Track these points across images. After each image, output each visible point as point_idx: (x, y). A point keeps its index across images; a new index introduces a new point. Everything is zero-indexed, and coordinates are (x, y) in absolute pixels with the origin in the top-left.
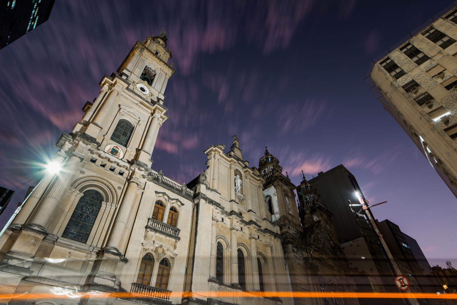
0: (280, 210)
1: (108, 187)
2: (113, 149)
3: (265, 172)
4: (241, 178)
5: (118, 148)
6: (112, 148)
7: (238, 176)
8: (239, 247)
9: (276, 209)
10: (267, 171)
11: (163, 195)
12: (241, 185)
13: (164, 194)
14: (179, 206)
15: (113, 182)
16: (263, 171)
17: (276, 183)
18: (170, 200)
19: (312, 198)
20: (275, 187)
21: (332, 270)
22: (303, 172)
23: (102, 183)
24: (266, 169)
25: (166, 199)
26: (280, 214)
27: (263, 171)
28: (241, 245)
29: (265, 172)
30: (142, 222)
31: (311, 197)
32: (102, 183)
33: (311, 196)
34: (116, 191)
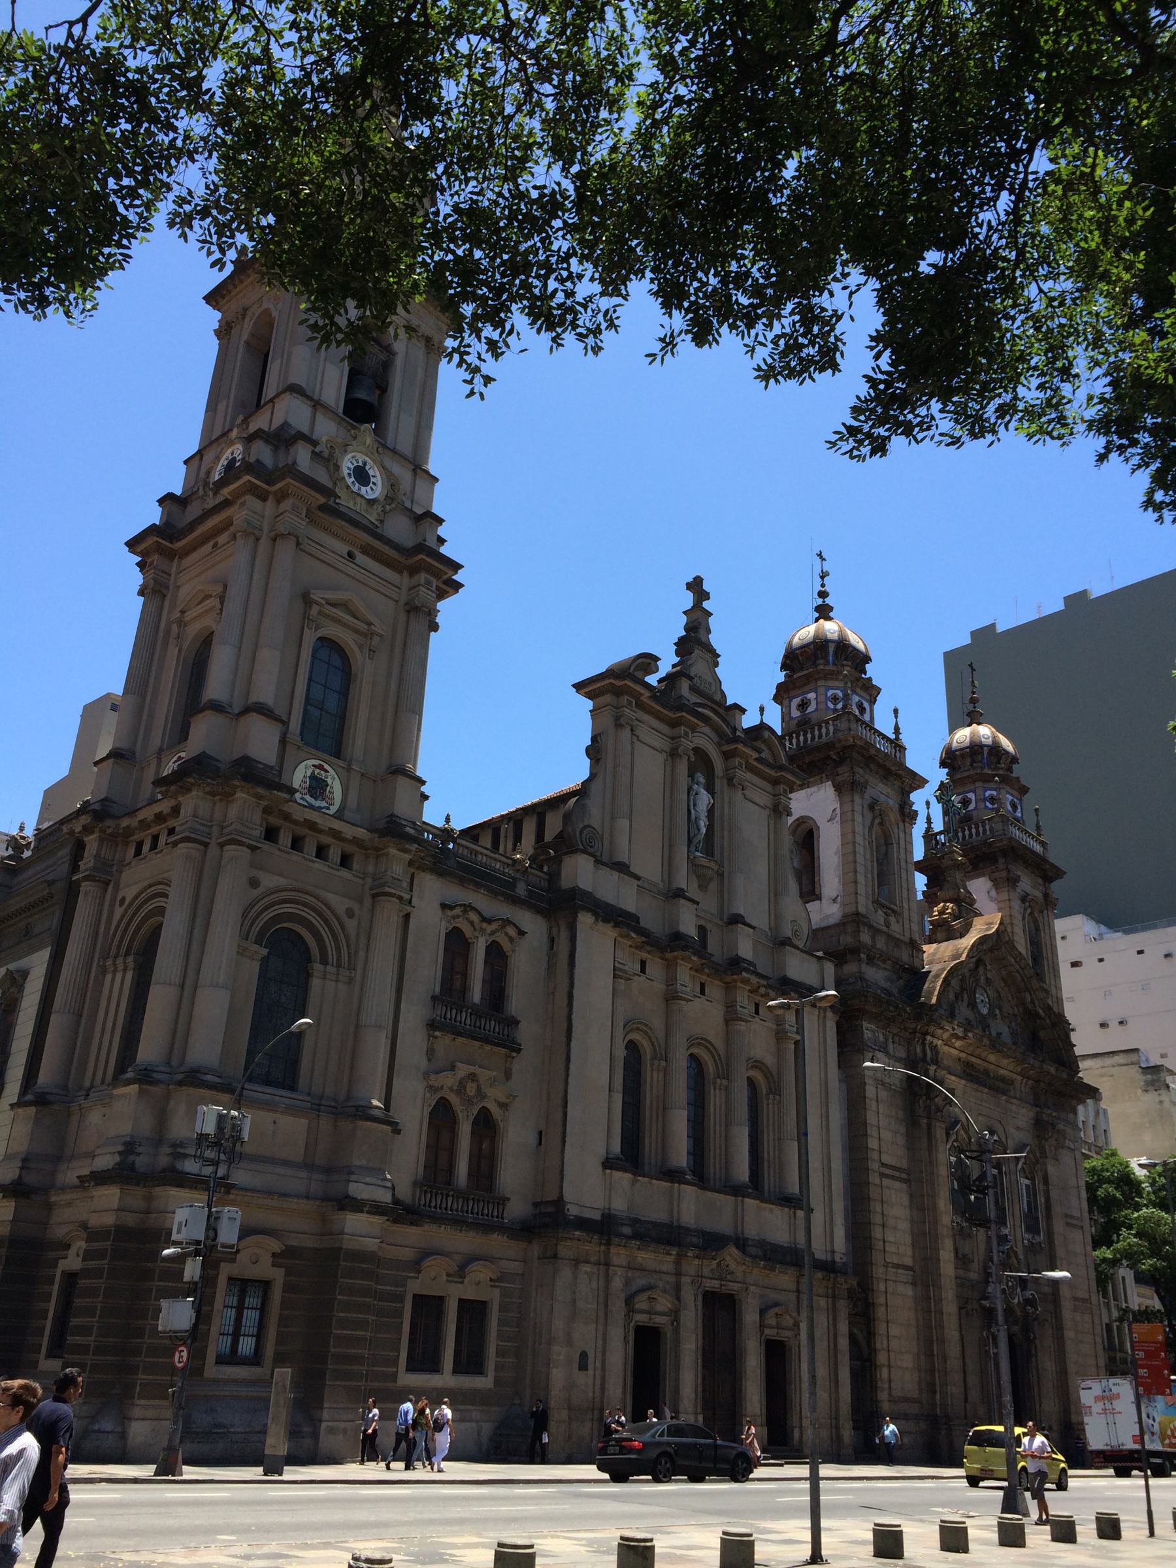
0: (844, 890)
1: (320, 914)
2: (313, 777)
3: (803, 705)
4: (710, 789)
5: (326, 771)
6: (309, 774)
7: (701, 778)
8: (691, 1051)
9: (831, 880)
11: (465, 912)
12: (711, 812)
13: (467, 908)
14: (511, 939)
15: (332, 898)
16: (796, 702)
17: (844, 773)
18: (484, 925)
19: (988, 804)
20: (838, 788)
21: (1004, 1098)
22: (973, 670)
23: (306, 905)
24: (812, 696)
25: (472, 923)
26: (843, 905)
27: (796, 702)
28: (699, 1044)
29: (803, 705)
30: (414, 1015)
31: (985, 800)
32: (306, 905)
33: (988, 794)
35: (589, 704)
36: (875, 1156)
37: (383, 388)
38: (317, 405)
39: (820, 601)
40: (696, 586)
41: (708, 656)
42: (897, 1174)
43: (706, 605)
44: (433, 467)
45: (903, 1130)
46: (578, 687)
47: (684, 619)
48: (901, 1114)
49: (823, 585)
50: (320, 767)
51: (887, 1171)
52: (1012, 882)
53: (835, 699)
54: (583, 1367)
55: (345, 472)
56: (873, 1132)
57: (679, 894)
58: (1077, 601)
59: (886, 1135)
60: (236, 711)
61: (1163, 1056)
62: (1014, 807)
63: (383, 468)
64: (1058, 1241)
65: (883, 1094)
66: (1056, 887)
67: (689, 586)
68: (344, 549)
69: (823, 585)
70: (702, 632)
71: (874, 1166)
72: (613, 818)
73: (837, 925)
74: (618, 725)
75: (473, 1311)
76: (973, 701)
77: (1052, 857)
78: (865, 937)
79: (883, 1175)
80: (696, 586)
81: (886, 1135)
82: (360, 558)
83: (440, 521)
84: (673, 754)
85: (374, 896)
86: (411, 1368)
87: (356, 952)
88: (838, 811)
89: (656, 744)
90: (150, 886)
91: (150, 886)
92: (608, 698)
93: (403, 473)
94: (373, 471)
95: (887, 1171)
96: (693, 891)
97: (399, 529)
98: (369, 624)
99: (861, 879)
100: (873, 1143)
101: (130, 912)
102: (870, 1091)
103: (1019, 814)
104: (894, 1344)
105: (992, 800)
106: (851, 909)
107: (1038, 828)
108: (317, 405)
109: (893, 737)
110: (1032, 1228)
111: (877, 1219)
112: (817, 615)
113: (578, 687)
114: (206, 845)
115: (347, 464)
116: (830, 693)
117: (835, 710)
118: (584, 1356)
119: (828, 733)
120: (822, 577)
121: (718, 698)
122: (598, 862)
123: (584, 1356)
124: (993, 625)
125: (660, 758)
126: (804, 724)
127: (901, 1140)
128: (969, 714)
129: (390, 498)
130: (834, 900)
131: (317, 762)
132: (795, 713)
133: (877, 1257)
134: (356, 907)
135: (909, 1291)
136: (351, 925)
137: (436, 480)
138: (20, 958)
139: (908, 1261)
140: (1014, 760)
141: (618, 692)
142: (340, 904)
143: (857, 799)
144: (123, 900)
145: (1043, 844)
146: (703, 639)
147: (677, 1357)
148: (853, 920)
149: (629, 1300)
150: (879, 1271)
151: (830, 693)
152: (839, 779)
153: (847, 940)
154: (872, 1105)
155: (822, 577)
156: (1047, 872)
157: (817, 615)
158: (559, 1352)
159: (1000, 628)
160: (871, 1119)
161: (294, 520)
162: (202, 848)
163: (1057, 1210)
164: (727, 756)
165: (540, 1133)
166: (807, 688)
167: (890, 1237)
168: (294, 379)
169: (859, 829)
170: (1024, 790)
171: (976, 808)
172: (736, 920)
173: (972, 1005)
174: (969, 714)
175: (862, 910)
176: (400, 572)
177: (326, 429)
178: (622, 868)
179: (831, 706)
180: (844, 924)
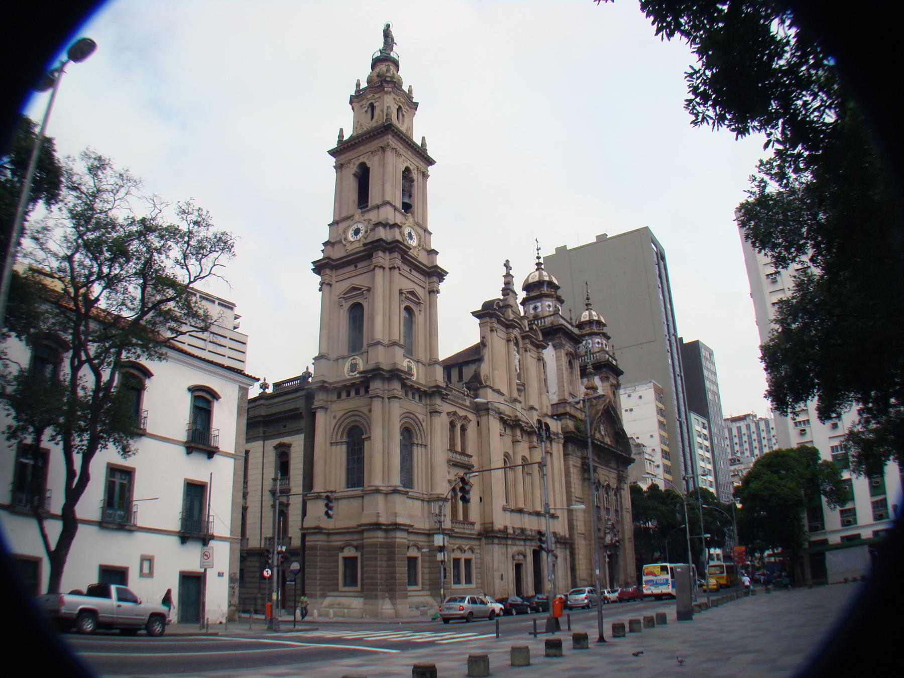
3: (535, 308)
4: (518, 352)
10: (539, 310)
12: (519, 362)
13: (455, 413)
16: (532, 306)
17: (557, 341)
24: (539, 304)
26: (559, 395)
27: (532, 306)
29: (535, 308)
33: (597, 340)
34: (422, 426)
35: (478, 321)
36: (573, 494)
37: (410, 196)
38: (395, 209)
39: (537, 261)
40: (507, 265)
41: (514, 295)
42: (579, 500)
43: (511, 272)
44: (430, 230)
45: (581, 483)
46: (474, 313)
47: (503, 279)
48: (580, 477)
49: (538, 254)
50: (409, 362)
51: (577, 499)
52: (607, 378)
53: (549, 306)
54: (502, 579)
55: (406, 235)
56: (573, 485)
57: (516, 400)
58: (602, 238)
59: (576, 486)
60: (386, 342)
61: (638, 438)
62: (606, 346)
63: (416, 232)
64: (624, 518)
65: (575, 470)
66: (620, 378)
67: (505, 265)
68: (407, 269)
69: (538, 254)
70: (511, 285)
71: (574, 498)
72: (493, 369)
73: (557, 404)
74: (492, 331)
75: (468, 562)
76: (588, 299)
77: (620, 367)
78: (568, 409)
79: (576, 501)
80: (507, 265)
81: (576, 486)
82: (414, 272)
83: (437, 253)
84: (508, 341)
85: (430, 413)
86: (454, 583)
87: (427, 434)
88: (555, 356)
89: (502, 336)
90: (350, 411)
91: (350, 411)
92: (488, 319)
93: (421, 232)
94: (413, 234)
95: (577, 499)
96: (520, 399)
97: (423, 258)
98: (419, 299)
99: (565, 385)
100: (573, 490)
101: (340, 421)
102: (572, 470)
103: (607, 349)
104: (580, 562)
105: (598, 343)
106: (561, 398)
107: (614, 354)
108: (395, 209)
109: (570, 321)
110: (617, 515)
111: (575, 518)
112: (536, 267)
113: (474, 313)
114: (383, 398)
115: (407, 231)
116: (547, 303)
117: (549, 311)
118: (502, 575)
119: (548, 322)
120: (538, 250)
121: (518, 313)
122: (494, 390)
123: (502, 575)
124: (566, 246)
125: (504, 342)
126: (536, 317)
127: (580, 488)
128: (587, 305)
129: (419, 245)
130: (555, 393)
131: (408, 360)
132: (532, 312)
133: (575, 531)
134: (425, 417)
135: (583, 542)
136: (424, 424)
137: (431, 234)
138: (284, 437)
139: (583, 532)
140: (605, 325)
141: (491, 316)
142: (421, 417)
143: (563, 351)
144: (335, 417)
145: (616, 360)
146: (512, 289)
147: (526, 573)
148: (563, 402)
149: (513, 557)
150: (576, 536)
151: (547, 303)
152: (555, 342)
153: (561, 410)
154: (572, 475)
155: (538, 250)
156: (617, 372)
157: (536, 267)
158: (497, 575)
159: (568, 248)
160: (572, 481)
161: (398, 262)
162: (381, 399)
163: (624, 507)
164: (524, 338)
165: (481, 498)
166: (536, 301)
167: (578, 524)
168: (388, 198)
169: (564, 364)
170: (608, 338)
171: (592, 347)
172: (532, 408)
173: (600, 432)
174: (587, 305)
175: (566, 398)
176: (425, 276)
177: (399, 219)
178: (499, 392)
179: (548, 309)
180: (560, 403)
